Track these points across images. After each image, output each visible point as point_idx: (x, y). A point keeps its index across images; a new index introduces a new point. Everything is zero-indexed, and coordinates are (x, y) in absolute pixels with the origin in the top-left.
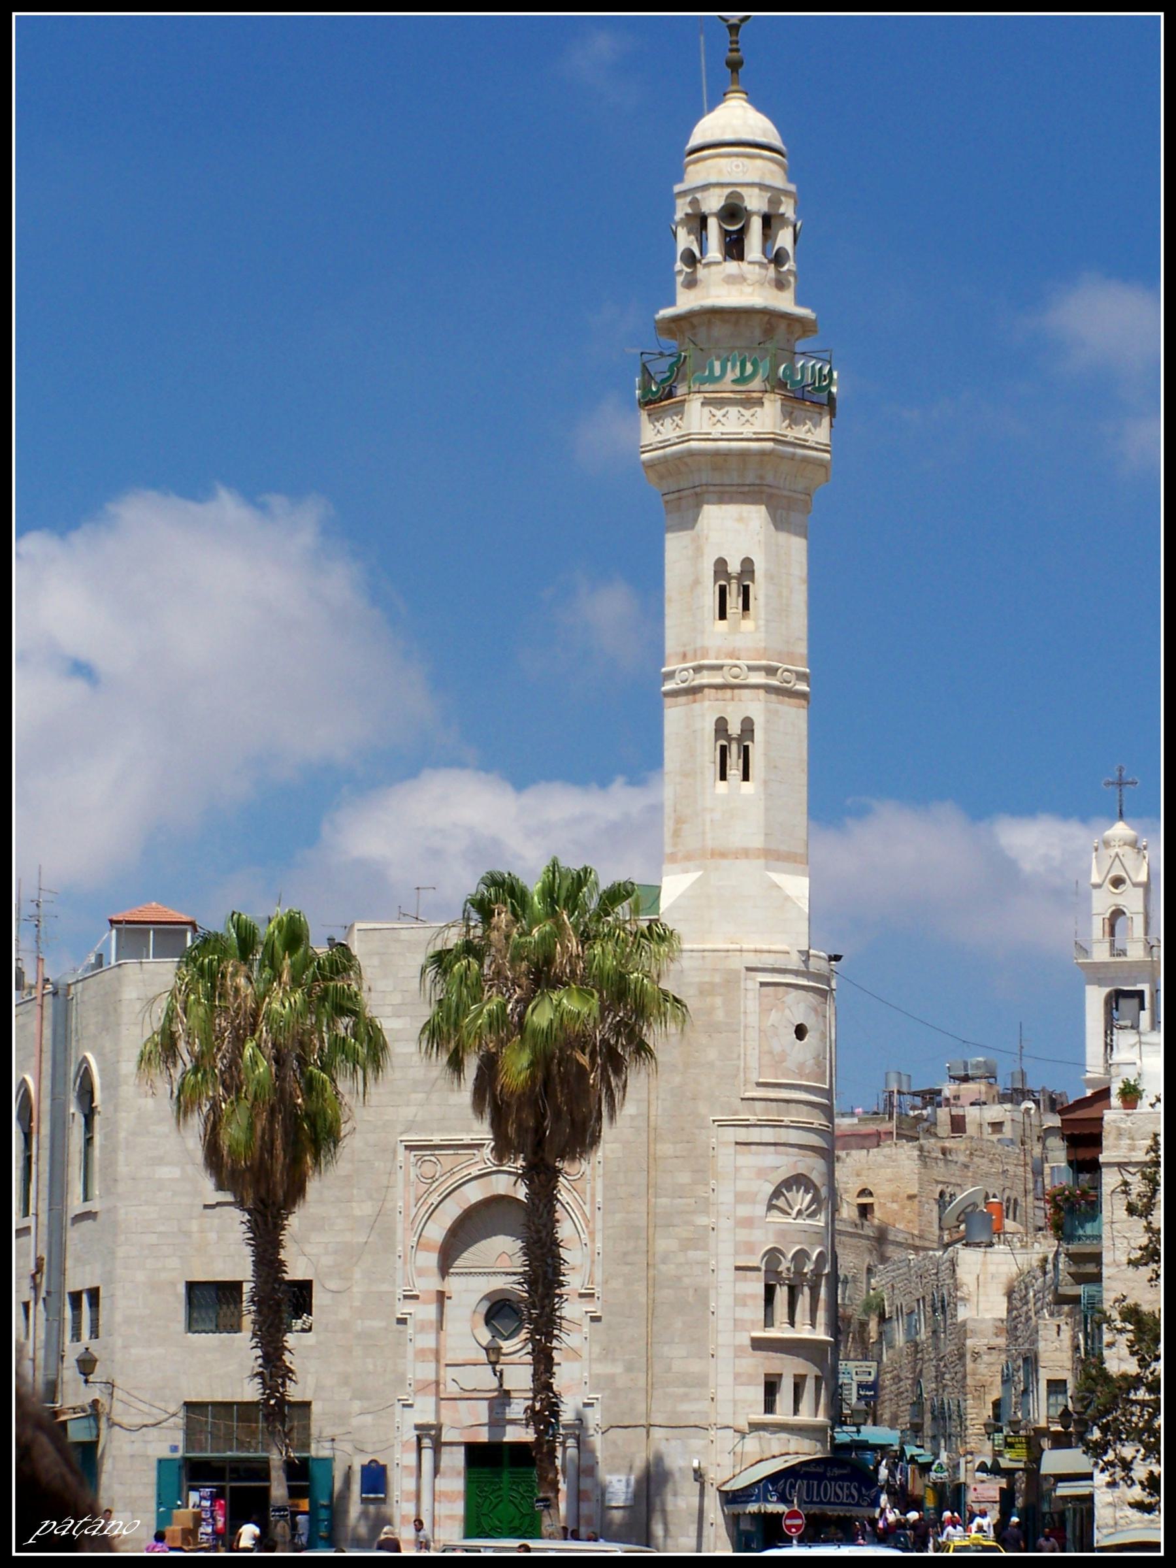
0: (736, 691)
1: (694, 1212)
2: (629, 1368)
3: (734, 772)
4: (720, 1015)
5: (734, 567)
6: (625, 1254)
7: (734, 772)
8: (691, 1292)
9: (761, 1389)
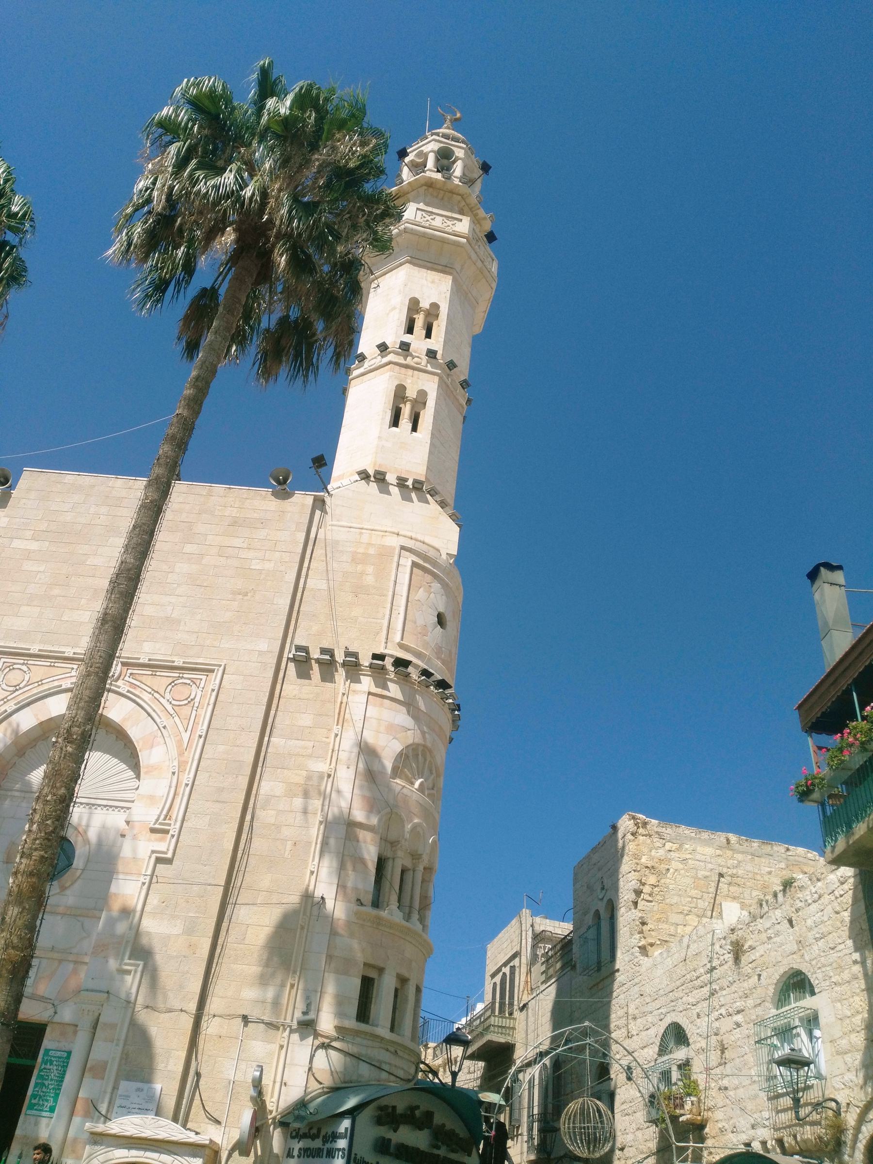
0: (416, 372)
1: (310, 756)
2: (189, 931)
3: (405, 423)
4: (370, 580)
5: (425, 304)
6: (221, 790)
7: (405, 423)
8: (289, 844)
9: (358, 982)
